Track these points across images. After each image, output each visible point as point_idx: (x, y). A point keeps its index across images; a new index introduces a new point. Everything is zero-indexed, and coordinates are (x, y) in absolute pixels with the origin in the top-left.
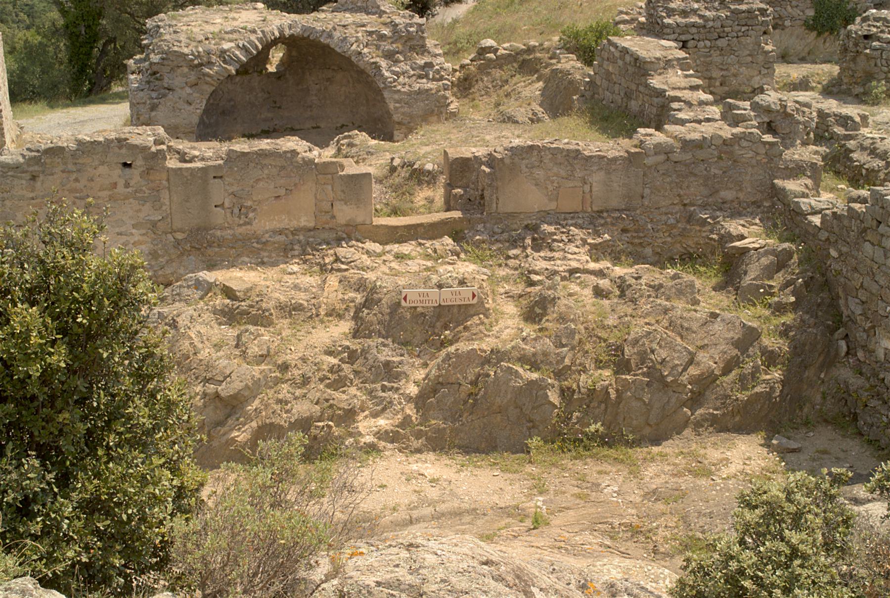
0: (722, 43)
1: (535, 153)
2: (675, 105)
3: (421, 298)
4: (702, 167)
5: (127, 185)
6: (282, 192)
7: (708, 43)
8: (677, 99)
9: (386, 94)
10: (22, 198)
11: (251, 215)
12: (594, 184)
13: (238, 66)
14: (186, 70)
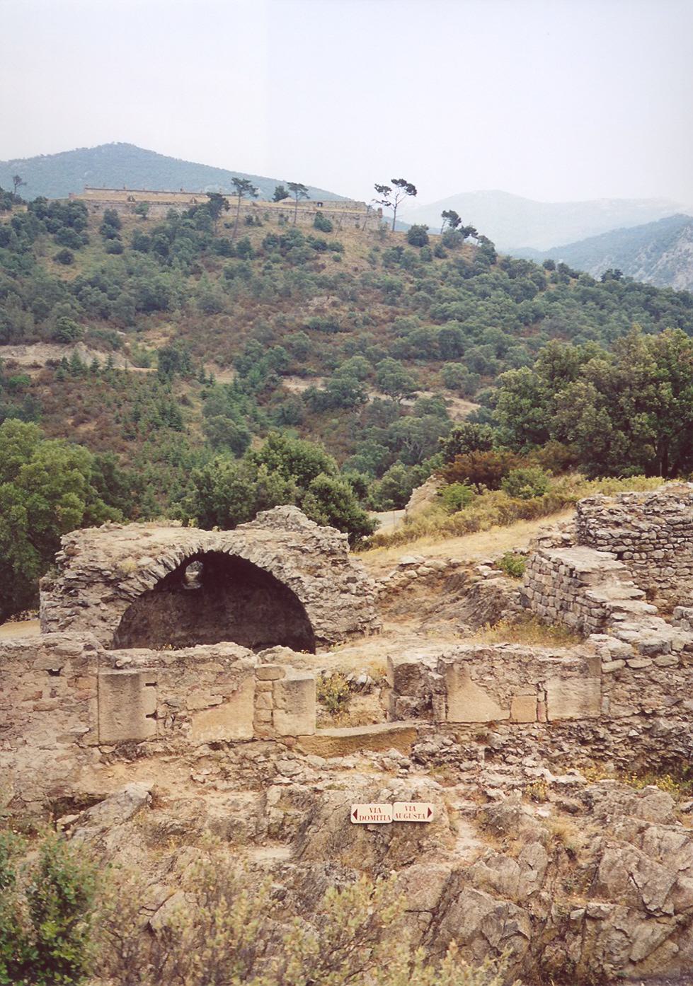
0: (659, 554)
2: (617, 616)
3: (373, 814)
4: (663, 673)
6: (219, 700)
7: (644, 555)
8: (619, 610)
9: (308, 609)
13: (156, 582)
14: (101, 586)
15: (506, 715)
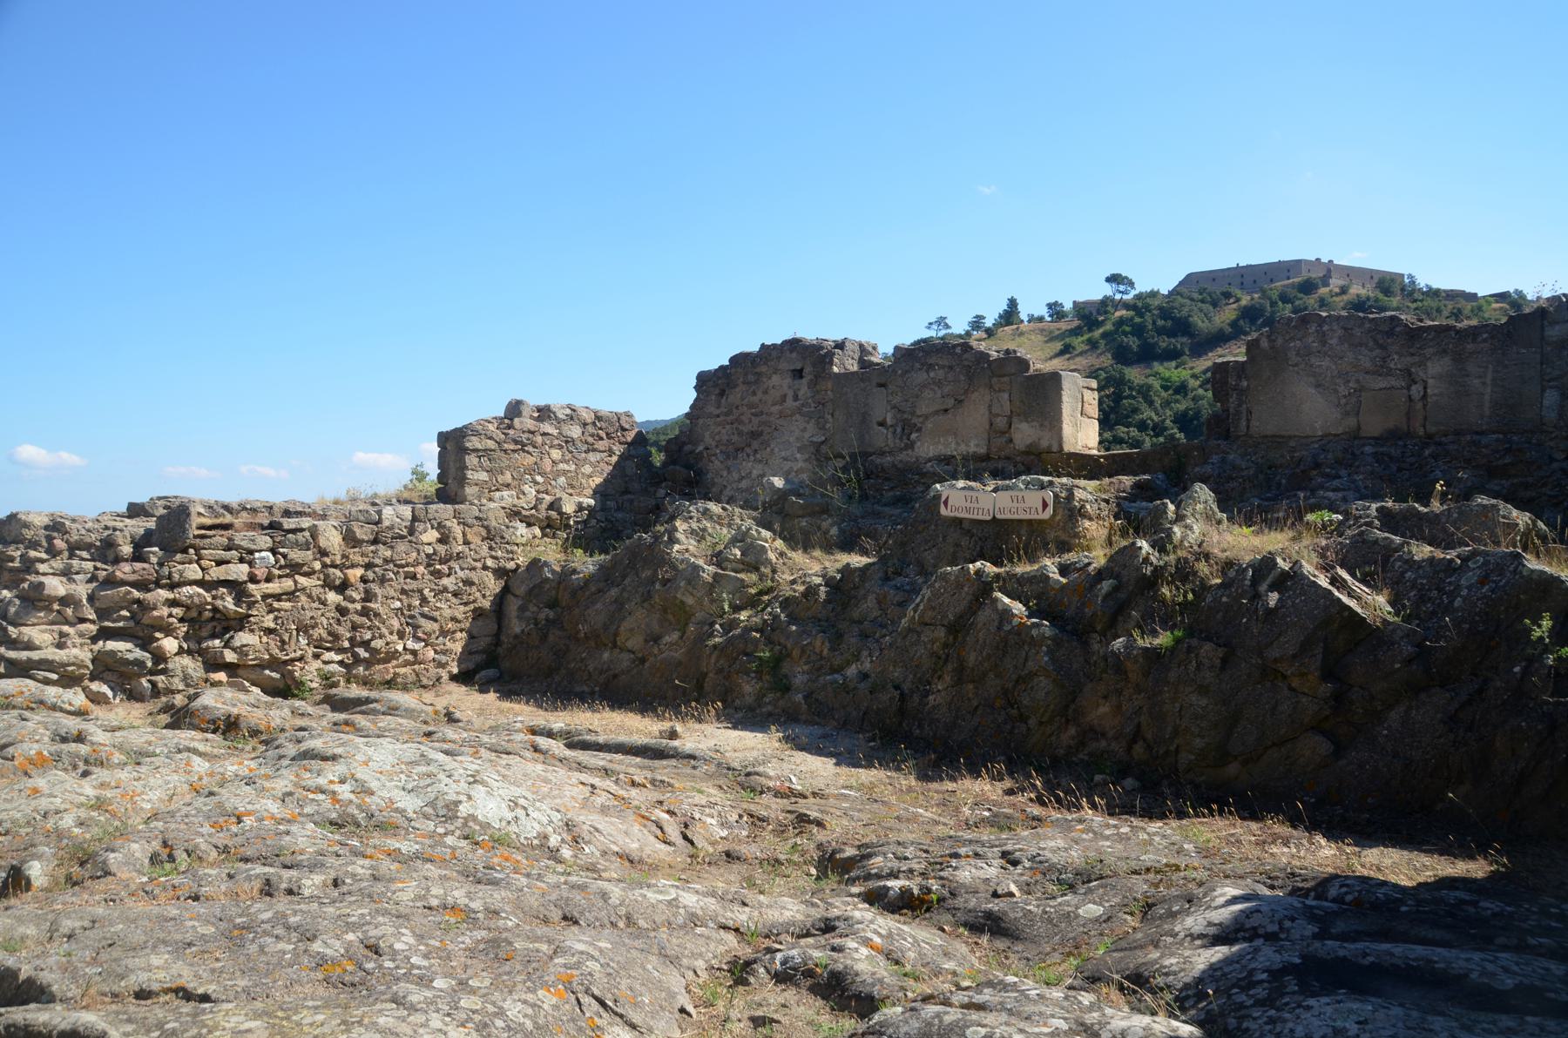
1: (1313, 328)
3: (968, 505)
5: (796, 398)
6: (950, 402)
10: (710, 416)
11: (914, 436)
12: (1431, 382)
15: (1351, 422)
